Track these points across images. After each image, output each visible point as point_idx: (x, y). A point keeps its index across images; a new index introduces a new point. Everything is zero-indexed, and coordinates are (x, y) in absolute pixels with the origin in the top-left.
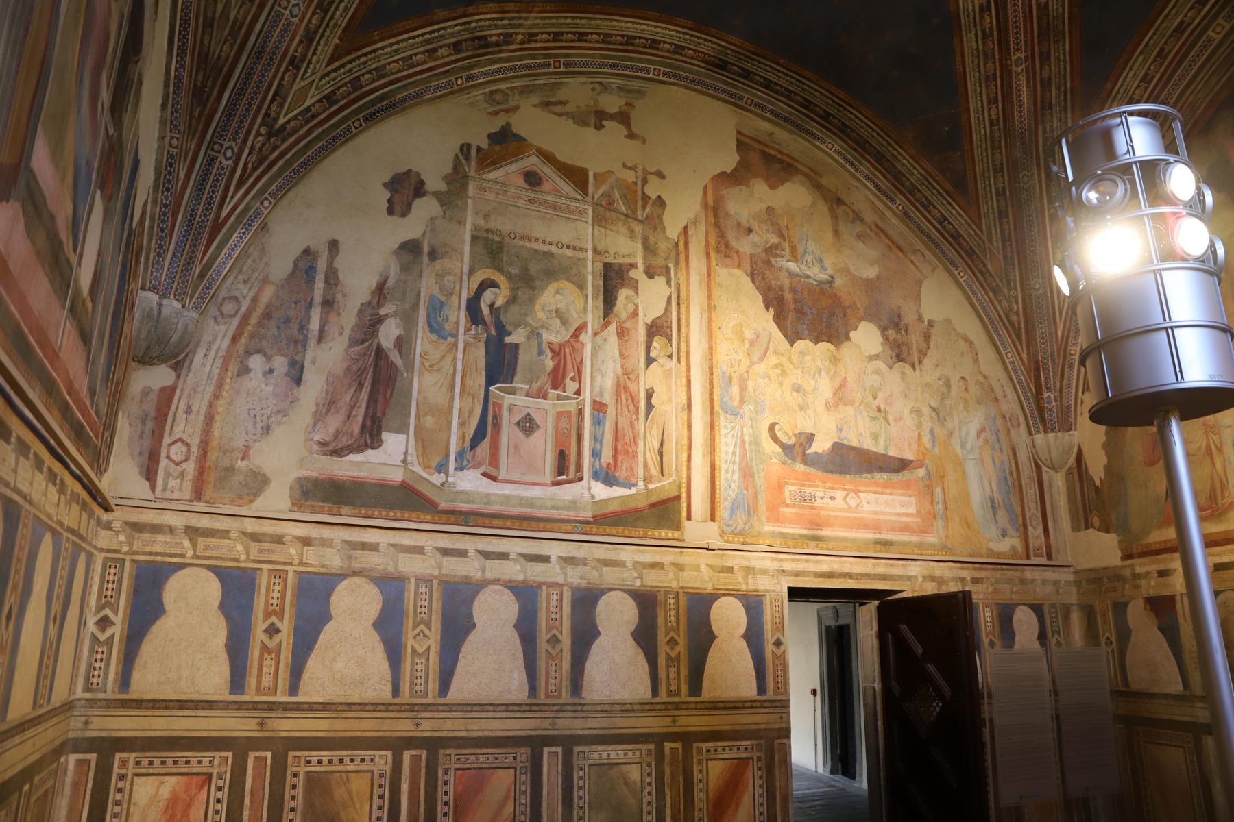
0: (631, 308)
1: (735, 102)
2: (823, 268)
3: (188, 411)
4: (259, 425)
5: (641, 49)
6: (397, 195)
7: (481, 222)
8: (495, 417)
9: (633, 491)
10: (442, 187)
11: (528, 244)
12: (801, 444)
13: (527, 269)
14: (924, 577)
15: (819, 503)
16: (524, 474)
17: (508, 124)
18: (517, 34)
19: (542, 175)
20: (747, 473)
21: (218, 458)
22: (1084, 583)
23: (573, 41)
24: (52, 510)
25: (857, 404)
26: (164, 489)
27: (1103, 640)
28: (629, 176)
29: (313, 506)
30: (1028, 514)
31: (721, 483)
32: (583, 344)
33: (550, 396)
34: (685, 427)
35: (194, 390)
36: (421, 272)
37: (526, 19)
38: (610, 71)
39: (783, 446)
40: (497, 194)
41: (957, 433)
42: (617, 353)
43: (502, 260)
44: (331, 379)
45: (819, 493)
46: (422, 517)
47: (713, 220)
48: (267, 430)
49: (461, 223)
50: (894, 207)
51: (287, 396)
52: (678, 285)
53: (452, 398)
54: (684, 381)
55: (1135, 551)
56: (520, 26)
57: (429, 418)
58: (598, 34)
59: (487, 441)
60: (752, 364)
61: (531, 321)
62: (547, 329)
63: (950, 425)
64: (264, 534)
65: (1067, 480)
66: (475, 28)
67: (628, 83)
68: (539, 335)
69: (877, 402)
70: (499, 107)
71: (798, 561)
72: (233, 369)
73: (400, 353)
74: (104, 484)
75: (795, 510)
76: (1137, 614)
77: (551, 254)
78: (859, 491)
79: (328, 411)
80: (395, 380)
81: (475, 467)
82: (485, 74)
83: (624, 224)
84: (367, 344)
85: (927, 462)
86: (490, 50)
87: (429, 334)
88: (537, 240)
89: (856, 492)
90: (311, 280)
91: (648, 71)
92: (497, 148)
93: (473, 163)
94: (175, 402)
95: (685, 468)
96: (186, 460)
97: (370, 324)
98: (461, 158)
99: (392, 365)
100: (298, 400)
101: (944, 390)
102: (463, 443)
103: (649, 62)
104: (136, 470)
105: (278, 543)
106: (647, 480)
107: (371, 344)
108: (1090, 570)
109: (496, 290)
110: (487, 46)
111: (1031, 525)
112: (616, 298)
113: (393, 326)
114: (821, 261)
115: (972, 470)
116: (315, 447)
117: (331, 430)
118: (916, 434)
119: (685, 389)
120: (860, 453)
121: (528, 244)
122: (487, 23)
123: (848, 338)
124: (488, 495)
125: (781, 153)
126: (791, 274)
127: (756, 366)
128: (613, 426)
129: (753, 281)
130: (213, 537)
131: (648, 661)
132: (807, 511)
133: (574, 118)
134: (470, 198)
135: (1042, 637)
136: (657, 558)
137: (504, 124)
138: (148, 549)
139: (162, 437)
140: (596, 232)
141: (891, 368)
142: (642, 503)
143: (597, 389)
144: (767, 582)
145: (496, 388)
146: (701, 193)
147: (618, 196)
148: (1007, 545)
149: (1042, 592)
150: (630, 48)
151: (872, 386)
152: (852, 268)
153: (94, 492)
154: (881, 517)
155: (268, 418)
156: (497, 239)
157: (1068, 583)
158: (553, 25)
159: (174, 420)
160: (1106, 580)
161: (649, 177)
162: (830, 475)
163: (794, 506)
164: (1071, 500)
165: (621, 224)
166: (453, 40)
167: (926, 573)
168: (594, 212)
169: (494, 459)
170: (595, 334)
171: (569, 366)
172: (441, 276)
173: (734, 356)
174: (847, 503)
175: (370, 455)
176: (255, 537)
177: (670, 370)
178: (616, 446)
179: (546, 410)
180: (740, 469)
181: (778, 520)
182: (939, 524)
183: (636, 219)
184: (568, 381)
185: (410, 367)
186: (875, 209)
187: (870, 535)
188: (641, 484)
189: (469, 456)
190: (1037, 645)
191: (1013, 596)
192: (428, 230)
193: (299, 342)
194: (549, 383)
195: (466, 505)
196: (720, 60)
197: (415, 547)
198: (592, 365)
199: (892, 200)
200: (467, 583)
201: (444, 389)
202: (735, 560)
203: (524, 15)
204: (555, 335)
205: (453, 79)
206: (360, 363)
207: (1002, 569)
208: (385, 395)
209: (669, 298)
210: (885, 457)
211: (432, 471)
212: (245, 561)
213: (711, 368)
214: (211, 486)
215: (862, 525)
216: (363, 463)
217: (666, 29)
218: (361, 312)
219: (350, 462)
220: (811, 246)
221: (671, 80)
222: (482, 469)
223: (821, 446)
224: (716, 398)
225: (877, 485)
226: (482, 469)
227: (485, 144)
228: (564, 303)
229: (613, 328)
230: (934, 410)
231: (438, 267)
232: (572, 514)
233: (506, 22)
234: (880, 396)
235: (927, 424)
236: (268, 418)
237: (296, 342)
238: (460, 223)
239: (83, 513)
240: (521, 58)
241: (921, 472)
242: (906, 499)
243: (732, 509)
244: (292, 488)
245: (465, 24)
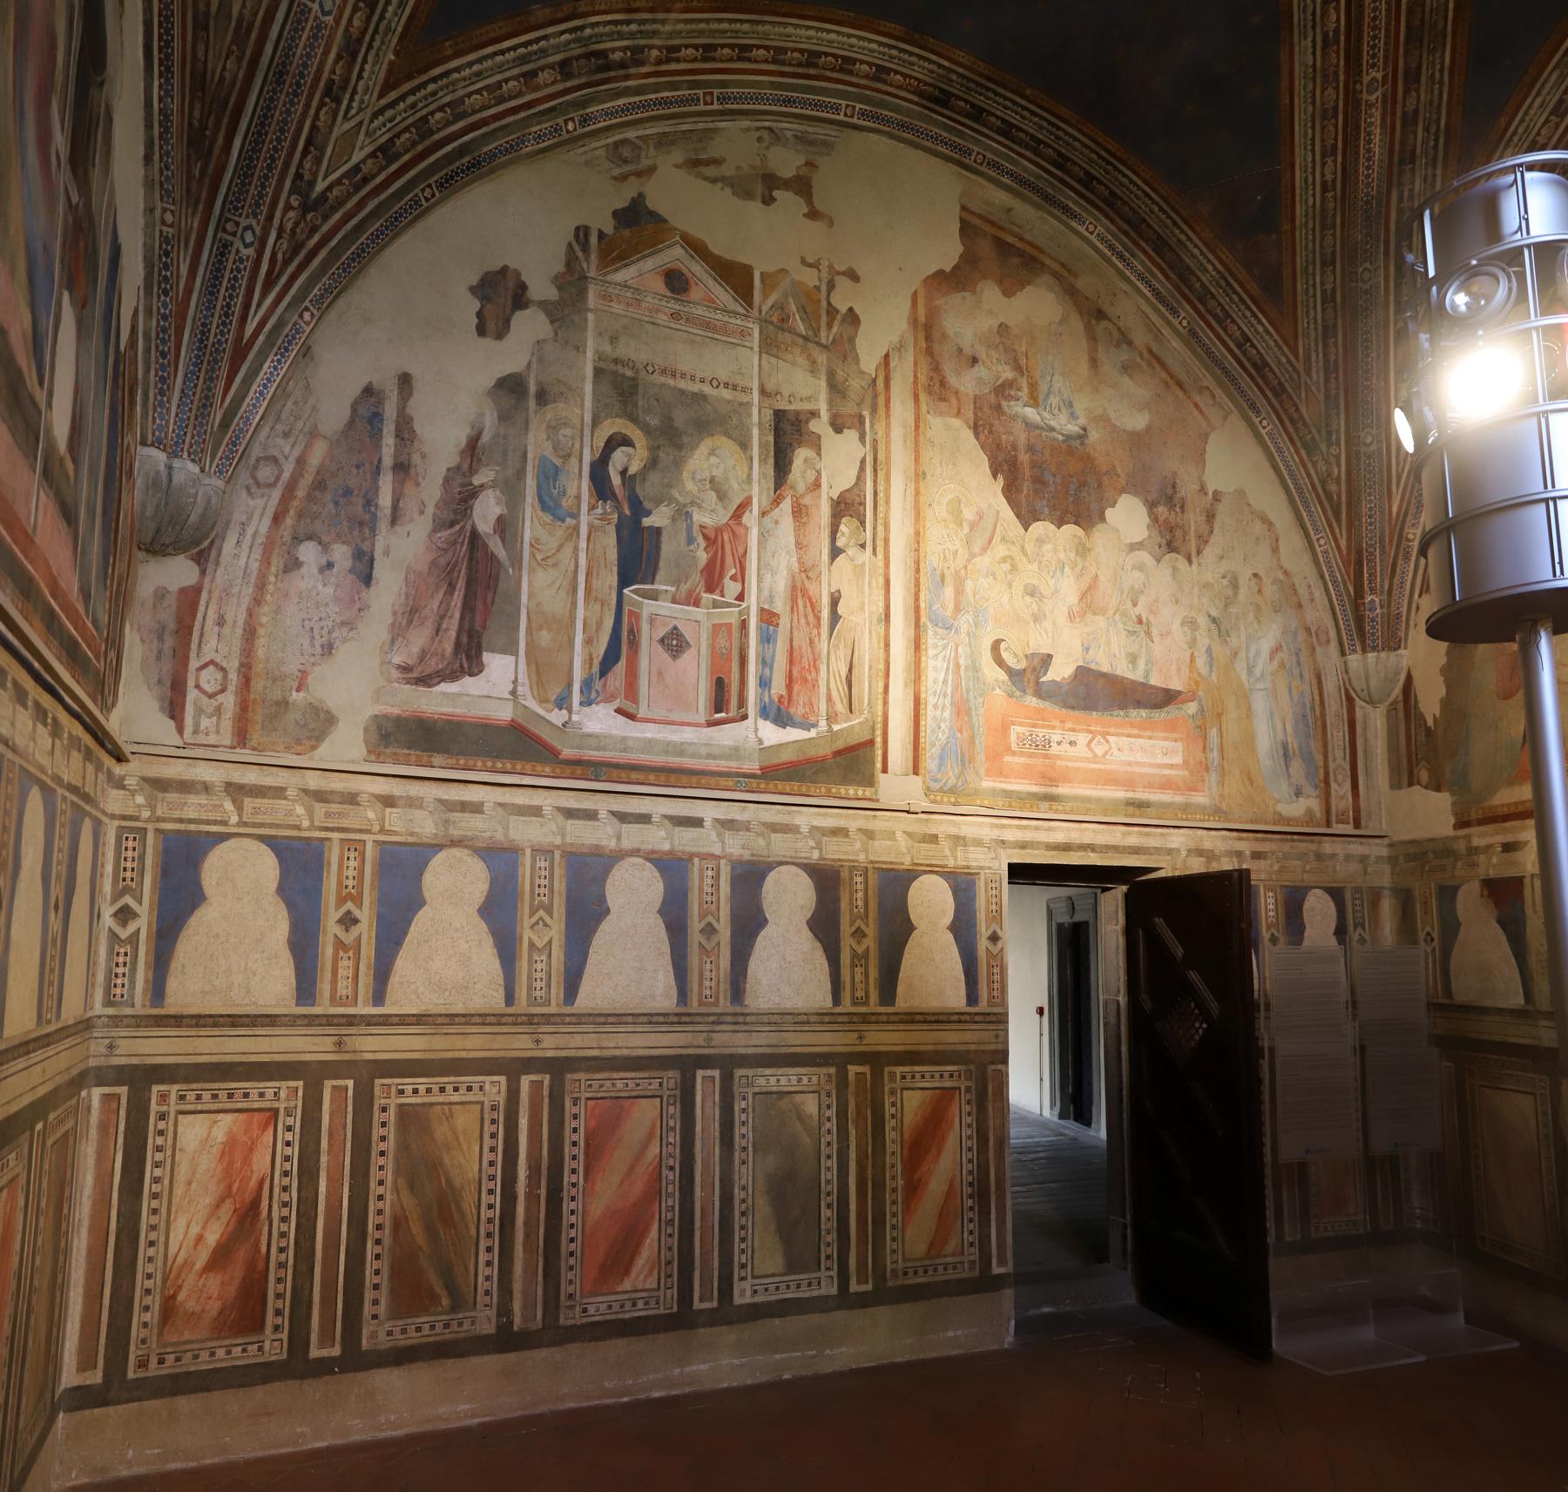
0: (811, 476)
1: (960, 160)
2: (1073, 416)
3: (221, 622)
4: (318, 643)
5: (828, 74)
6: (489, 306)
7: (607, 348)
8: (631, 631)
9: (813, 733)
10: (552, 294)
11: (671, 382)
12: (1034, 669)
13: (671, 419)
14: (1189, 851)
15: (1055, 749)
16: (670, 710)
17: (641, 195)
18: (651, 47)
19: (689, 275)
20: (962, 710)
21: (265, 688)
22: (1401, 859)
23: (731, 60)
24: (45, 761)
25: (1111, 612)
26: (196, 732)
27: (1421, 936)
28: (810, 278)
29: (395, 754)
30: (1332, 766)
31: (928, 723)
32: (747, 528)
33: (703, 601)
34: (882, 645)
35: (226, 592)
36: (527, 422)
37: (663, 22)
39: (1010, 672)
40: (628, 305)
41: (1242, 654)
42: (792, 540)
43: (636, 404)
44: (411, 577)
45: (1056, 738)
46: (539, 768)
47: (924, 345)
48: (328, 649)
49: (580, 348)
50: (1175, 322)
51: (353, 601)
52: (875, 442)
53: (574, 604)
54: (881, 580)
55: (1474, 816)
56: (654, 33)
57: (544, 633)
58: (766, 48)
59: (621, 666)
60: (972, 556)
61: (677, 495)
62: (700, 507)
63: (1234, 642)
64: (332, 792)
65: (1388, 719)
66: (591, 37)
67: (810, 129)
68: (688, 515)
69: (1137, 610)
70: (627, 168)
71: (1025, 827)
72: (277, 562)
73: (503, 540)
74: (113, 723)
75: (1022, 760)
76: (1470, 903)
77: (700, 397)
78: (1108, 734)
79: (410, 622)
80: (497, 578)
81: (606, 701)
82: (607, 114)
83: (802, 352)
84: (457, 527)
85: (1200, 693)
86: (613, 74)
87: (540, 513)
88: (683, 376)
89: (1105, 735)
90: (376, 434)
91: (837, 108)
92: (626, 233)
93: (594, 257)
94: (201, 608)
95: (880, 702)
96: (222, 691)
97: (461, 499)
98: (577, 248)
99: (493, 558)
100: (368, 607)
101: (1230, 592)
102: (591, 668)
104: (155, 705)
105: (351, 803)
106: (831, 718)
107: (463, 527)
108: (1411, 842)
109: (629, 449)
110: (609, 67)
111: (1336, 781)
112: (791, 462)
113: (492, 501)
114: (1071, 405)
115: (1260, 704)
116: (395, 674)
117: (415, 649)
118: (1188, 654)
119: (882, 592)
120: (1112, 680)
121: (671, 382)
122: (607, 29)
123: (1102, 519)
124: (624, 739)
125: (1021, 239)
126: (1029, 425)
127: (976, 560)
128: (787, 646)
129: (977, 435)
130: (264, 796)
131: (828, 959)
132: (1039, 761)
133: (733, 186)
134: (591, 310)
135: (1341, 932)
136: (842, 823)
137: (635, 195)
138: (177, 814)
139: (187, 658)
140: (764, 363)
141: (1158, 561)
142: (825, 750)
143: (766, 592)
144: (982, 856)
145: (631, 591)
146: (908, 303)
147: (794, 308)
148: (1299, 807)
149: (1344, 872)
150: (812, 71)
151: (1133, 588)
152: (1112, 415)
153: (100, 736)
154: (1136, 769)
155: (330, 633)
156: (629, 373)
157: (1379, 859)
158: (702, 32)
159: (202, 635)
160: (1431, 856)
161: (838, 279)
162: (1071, 712)
163: (1022, 754)
164: (1392, 746)
165: (797, 351)
166: (558, 58)
167: (1192, 845)
168: (761, 333)
169: (631, 691)
170: (763, 514)
171: (729, 560)
172: (554, 428)
173: (949, 545)
174: (1091, 750)
175: (468, 684)
176: (320, 796)
177: (863, 565)
178: (791, 671)
179: (697, 621)
180: (952, 703)
181: (1001, 774)
182: (1213, 778)
183: (818, 344)
184: (727, 581)
185: (517, 561)
186: (1150, 326)
187: (1120, 794)
188: (823, 724)
189: (598, 685)
190: (1333, 941)
191: (1305, 876)
192: (534, 359)
193: (366, 524)
194: (702, 583)
195: (596, 753)
196: (941, 90)
197: (530, 807)
198: (759, 559)
199: (1174, 312)
200: (599, 855)
201: (563, 593)
202: (942, 826)
203: (660, 16)
204: (709, 516)
205: (560, 121)
206: (450, 554)
207: (1293, 841)
208: (485, 599)
209: (863, 462)
210: (1145, 686)
211: (550, 706)
212: (309, 829)
213: (917, 563)
214: (258, 727)
215: (1110, 779)
216: (459, 695)
217: (863, 39)
218: (447, 480)
219: (443, 693)
220: (1058, 382)
222: (616, 704)
223: (1060, 671)
224: (922, 605)
225: (1132, 725)
226: (616, 704)
227: (609, 228)
228: (721, 469)
229: (786, 505)
230: (1214, 620)
231: (549, 416)
232: (732, 765)
233: (634, 27)
234: (1142, 600)
235: (1203, 641)
236: (330, 633)
237: (361, 524)
238: (577, 348)
239: (88, 764)
240: (656, 88)
241: (1192, 708)
242: (1170, 744)
243: (941, 758)
244: (366, 730)
245: (575, 29)
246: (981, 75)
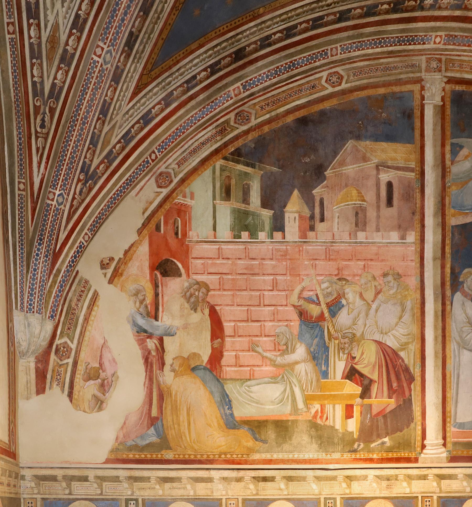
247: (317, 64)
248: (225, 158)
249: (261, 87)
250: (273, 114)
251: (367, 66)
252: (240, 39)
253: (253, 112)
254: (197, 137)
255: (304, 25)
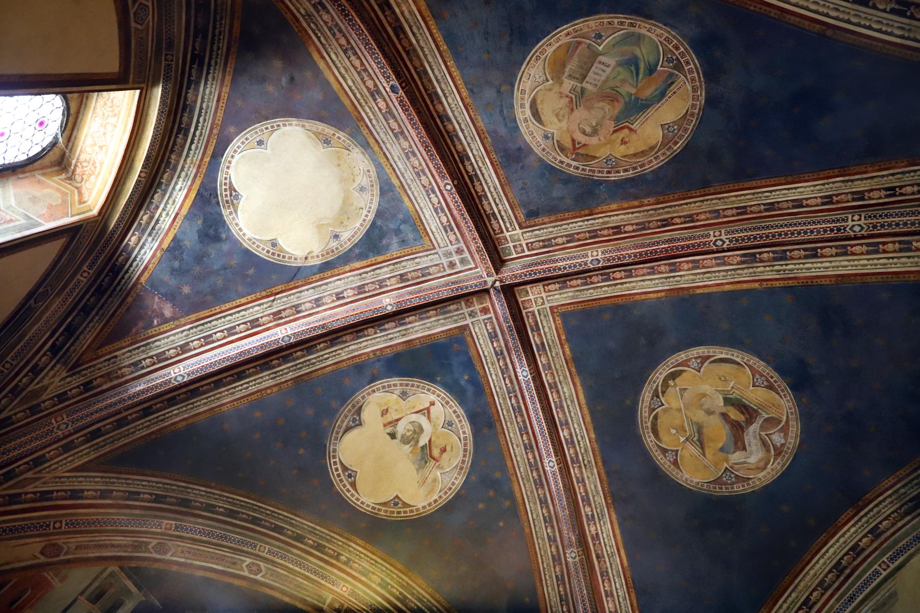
5: (855, 563)
38: (854, 605)
67: (878, 597)
91: (877, 573)
103: (871, 565)
150: (847, 571)
221: (902, 559)
246: (908, 475)
247: (245, 549)
248: (122, 568)
249: (189, 535)
250: (189, 561)
251: (285, 575)
252: (189, 493)
253: (173, 550)
254: (112, 538)
255: (244, 516)
